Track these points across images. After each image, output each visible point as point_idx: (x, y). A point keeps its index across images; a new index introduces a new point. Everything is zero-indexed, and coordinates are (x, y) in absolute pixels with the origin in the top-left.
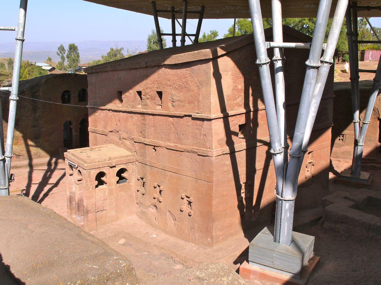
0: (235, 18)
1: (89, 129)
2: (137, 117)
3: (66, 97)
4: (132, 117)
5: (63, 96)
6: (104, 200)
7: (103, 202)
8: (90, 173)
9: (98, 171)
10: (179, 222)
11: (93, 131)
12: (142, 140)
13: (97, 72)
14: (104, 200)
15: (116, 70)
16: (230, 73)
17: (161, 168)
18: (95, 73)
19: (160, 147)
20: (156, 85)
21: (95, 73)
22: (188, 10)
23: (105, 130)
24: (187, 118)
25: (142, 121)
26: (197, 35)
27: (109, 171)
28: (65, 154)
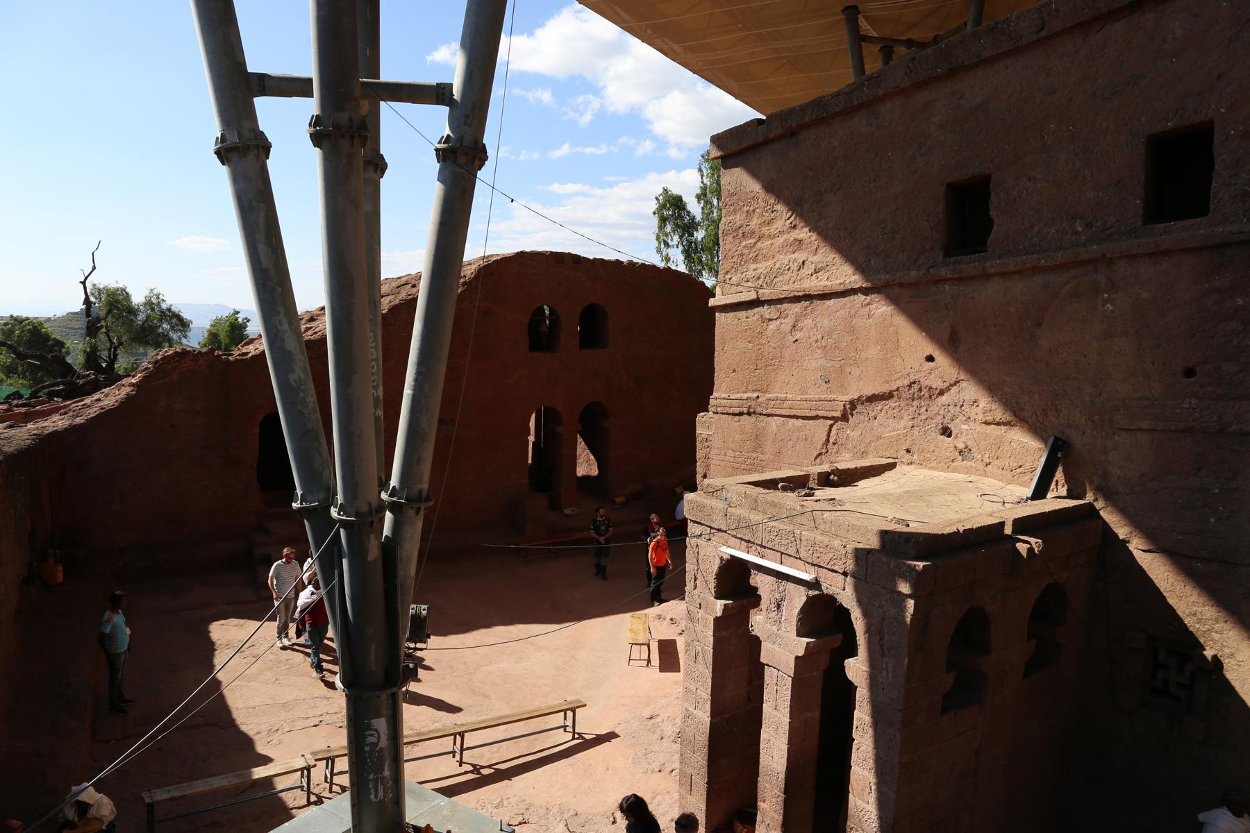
11: (737, 411)
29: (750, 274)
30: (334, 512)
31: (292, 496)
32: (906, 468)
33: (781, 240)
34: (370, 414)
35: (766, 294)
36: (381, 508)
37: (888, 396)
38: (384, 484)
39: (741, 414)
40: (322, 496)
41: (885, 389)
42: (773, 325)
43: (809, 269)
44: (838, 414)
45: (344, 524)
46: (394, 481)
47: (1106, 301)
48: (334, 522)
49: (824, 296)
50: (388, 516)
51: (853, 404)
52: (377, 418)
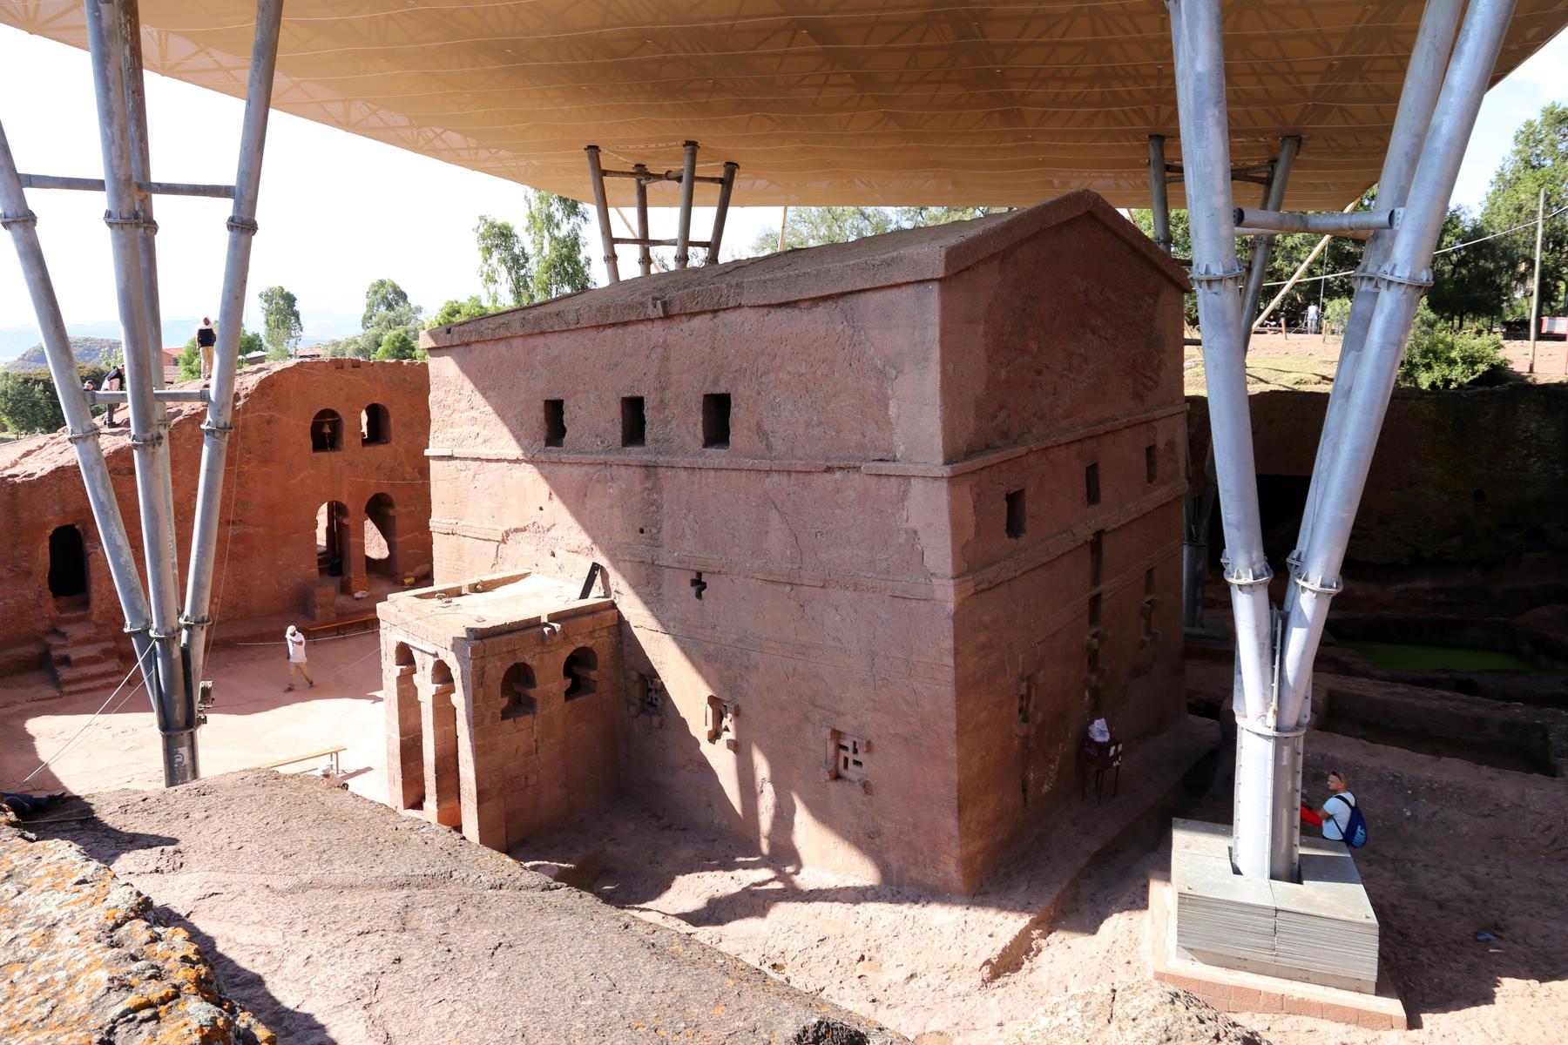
0: (786, 204)
1: (431, 524)
3: (327, 430)
5: (316, 430)
13: (468, 344)
15: (542, 333)
16: (981, 328)
18: (457, 345)
21: (457, 345)
22: (697, 174)
26: (714, 246)
29: (449, 436)
30: (152, 633)
31: (123, 624)
32: (536, 575)
33: (465, 415)
34: (171, 572)
35: (458, 452)
36: (180, 629)
37: (524, 530)
38: (180, 613)
39: (448, 534)
40: (143, 623)
41: (521, 525)
42: (463, 474)
43: (480, 440)
44: (500, 539)
45: (158, 639)
46: (187, 612)
47: (610, 487)
48: (152, 639)
49: (488, 460)
50: (184, 633)
51: (507, 533)
52: (174, 575)
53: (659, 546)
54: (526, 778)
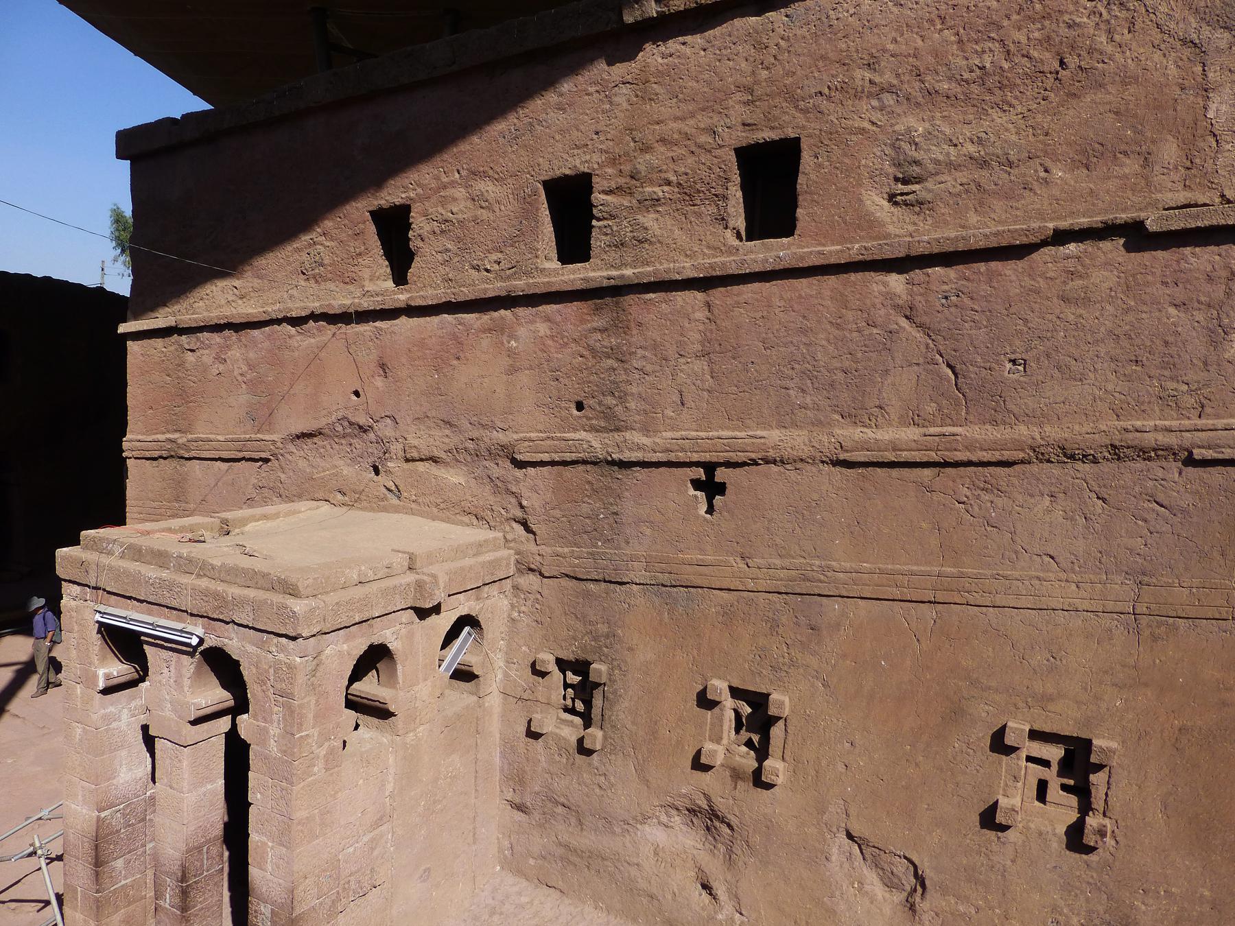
1: (125, 445)
2: (548, 319)
4: (497, 329)
6: (378, 823)
7: (372, 840)
8: (323, 657)
9: (360, 647)
10: (966, 899)
11: (156, 453)
12: (598, 444)
14: (378, 823)
17: (763, 585)
19: (767, 461)
20: (738, 112)
23: (260, 436)
24: (1072, 247)
25: (598, 336)
27: (410, 635)
28: (63, 558)
53: (618, 430)
54: (372, 870)
